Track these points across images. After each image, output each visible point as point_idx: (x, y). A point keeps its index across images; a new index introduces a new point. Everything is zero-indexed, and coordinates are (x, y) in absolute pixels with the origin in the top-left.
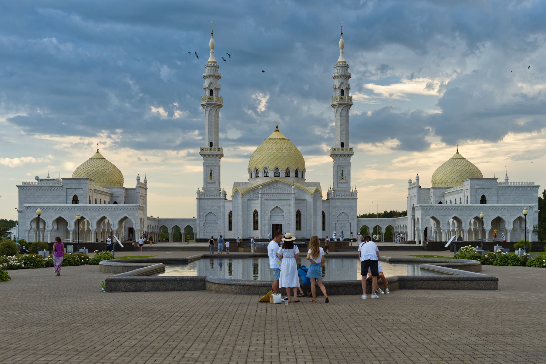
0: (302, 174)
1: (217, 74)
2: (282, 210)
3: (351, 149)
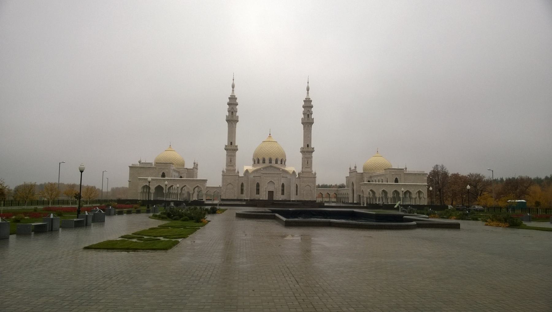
2: (274, 183)
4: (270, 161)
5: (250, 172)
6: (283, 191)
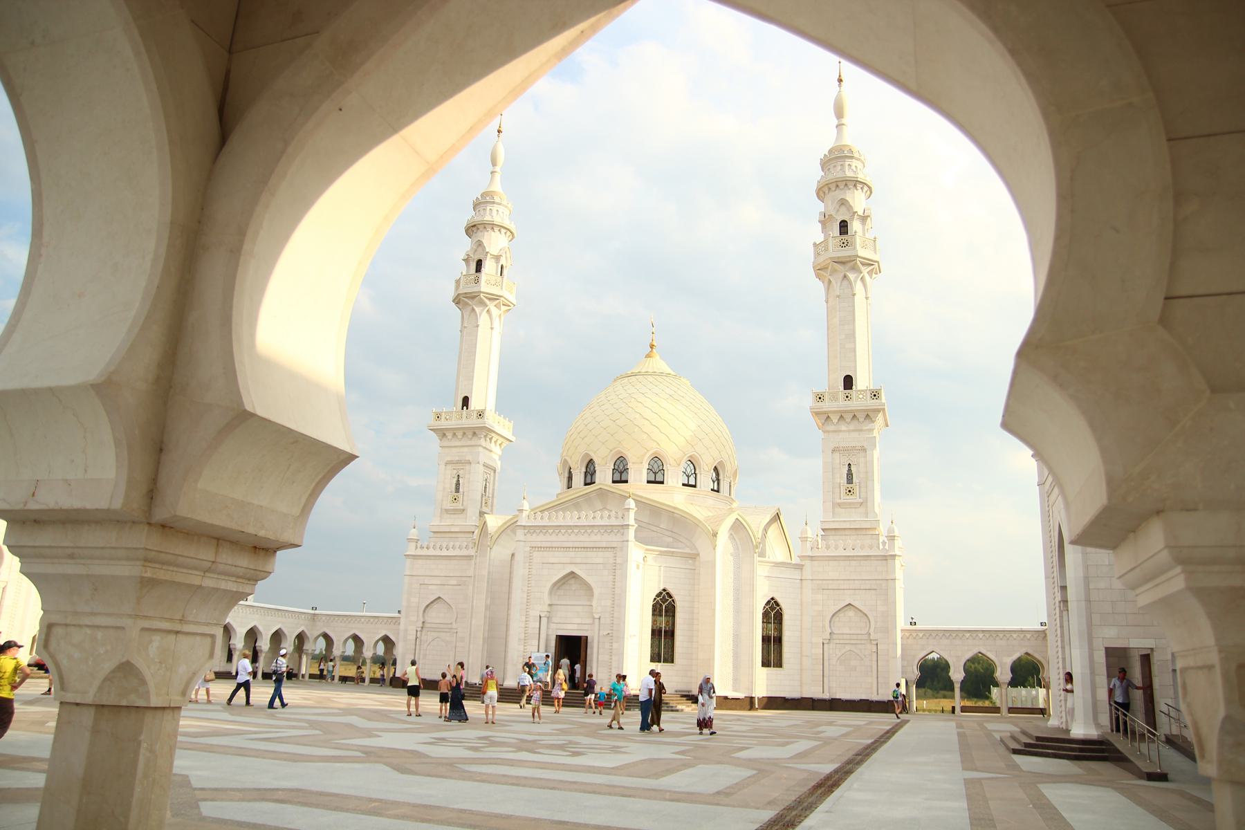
2: (588, 588)
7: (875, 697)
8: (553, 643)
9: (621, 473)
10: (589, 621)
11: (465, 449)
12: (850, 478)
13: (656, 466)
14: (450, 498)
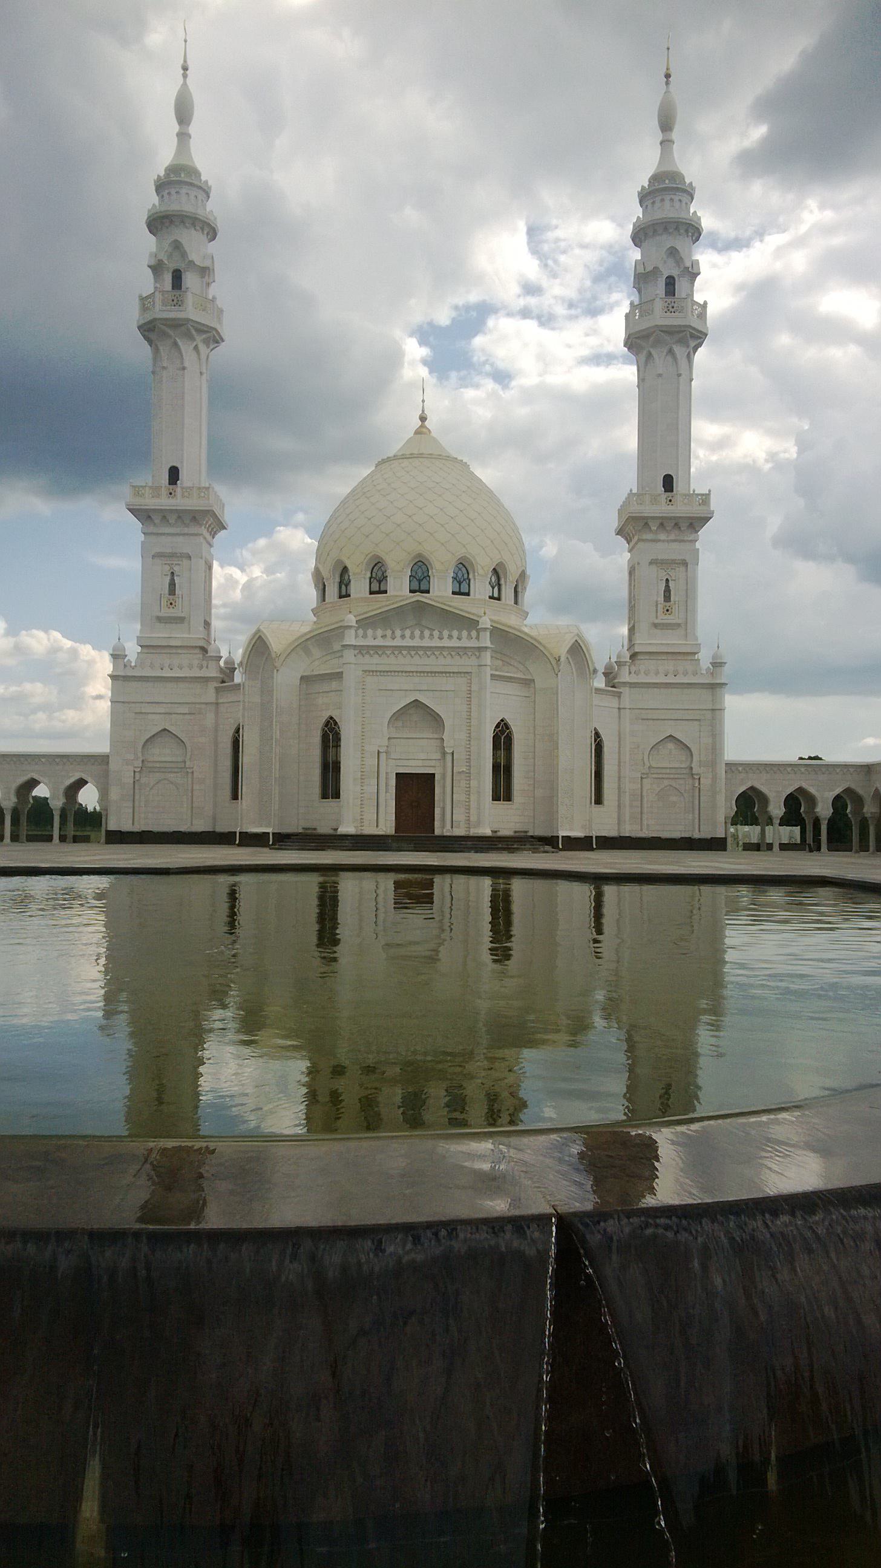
0: (516, 592)
1: (200, 212)
2: (436, 720)
3: (705, 499)
4: (420, 579)
5: (277, 644)
6: (502, 773)
7: (696, 835)
8: (393, 782)
9: (420, 581)
10: (438, 756)
11: (180, 539)
12: (667, 596)
13: (460, 575)
14: (164, 602)
